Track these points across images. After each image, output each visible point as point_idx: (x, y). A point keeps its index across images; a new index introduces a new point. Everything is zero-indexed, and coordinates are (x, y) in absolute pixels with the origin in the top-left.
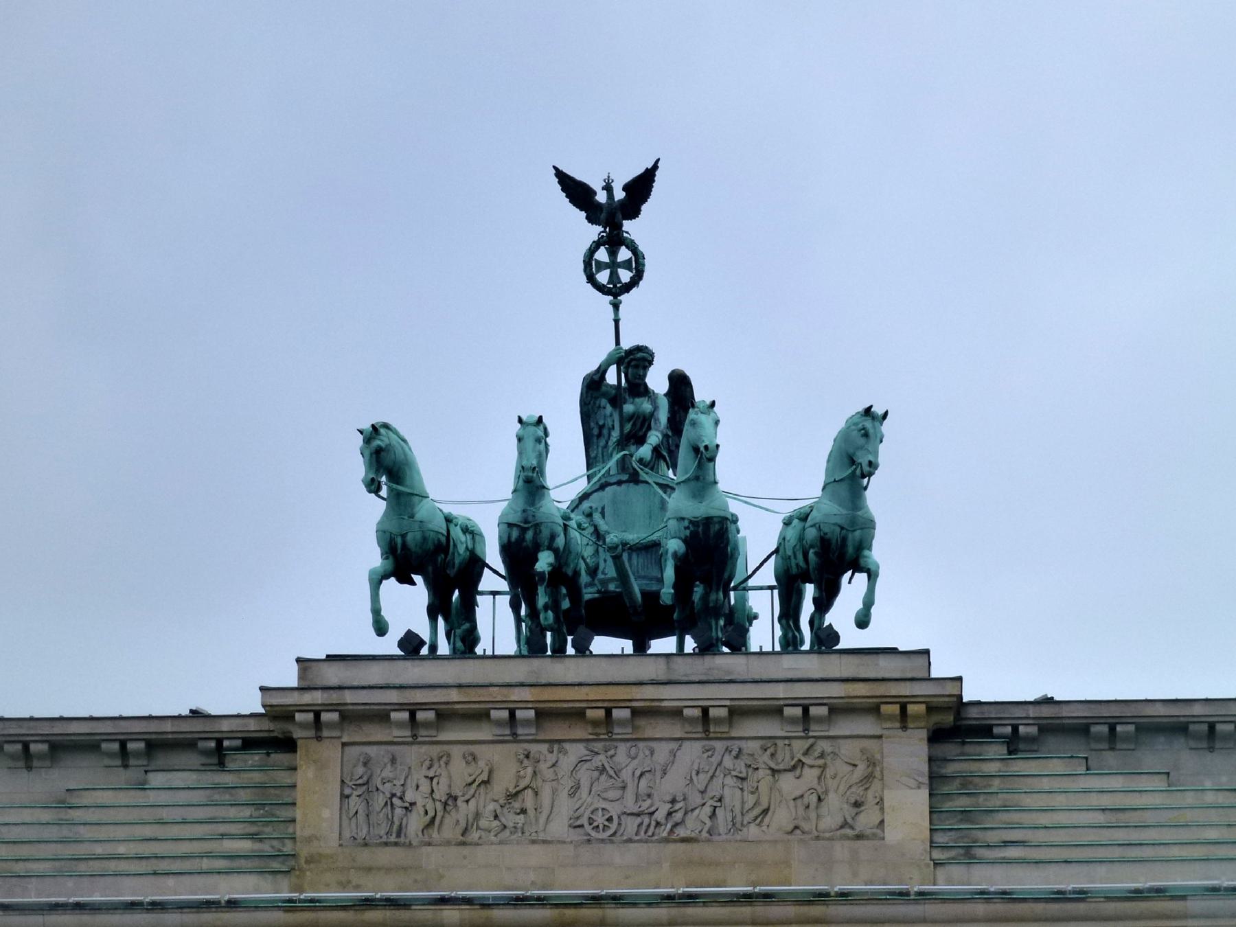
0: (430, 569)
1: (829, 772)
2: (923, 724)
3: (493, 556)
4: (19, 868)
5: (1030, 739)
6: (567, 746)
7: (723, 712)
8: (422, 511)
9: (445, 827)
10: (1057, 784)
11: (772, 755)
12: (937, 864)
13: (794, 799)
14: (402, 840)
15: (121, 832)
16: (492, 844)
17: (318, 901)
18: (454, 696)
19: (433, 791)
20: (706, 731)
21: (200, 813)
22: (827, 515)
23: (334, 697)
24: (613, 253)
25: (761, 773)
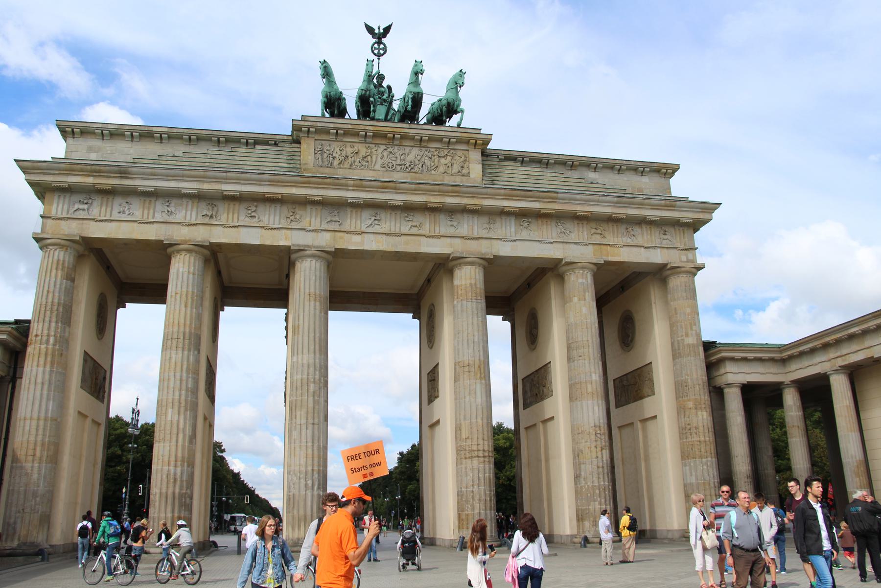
0: (337, 103)
2: (480, 147)
4: (217, 165)
6: (380, 146)
7: (427, 138)
11: (439, 153)
16: (359, 169)
18: (350, 126)
19: (341, 154)
23: (314, 124)
24: (379, 46)
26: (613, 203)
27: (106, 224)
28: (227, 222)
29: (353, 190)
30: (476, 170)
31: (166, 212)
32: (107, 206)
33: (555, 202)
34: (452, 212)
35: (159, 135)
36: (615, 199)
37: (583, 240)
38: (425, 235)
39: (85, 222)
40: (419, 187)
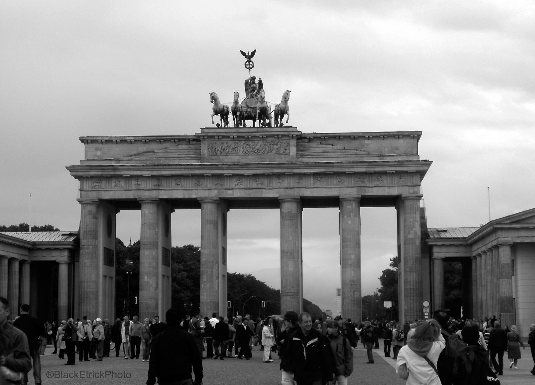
1: (282, 145)
3: (230, 111)
4: (159, 159)
5: (312, 139)
6: (242, 141)
8: (219, 105)
9: (223, 153)
10: (316, 146)
11: (273, 143)
12: (297, 158)
13: (276, 149)
14: (217, 155)
15: (174, 153)
17: (205, 164)
19: (221, 148)
20: (263, 139)
21: (187, 151)
22: (282, 106)
24: (249, 63)
25: (271, 145)
26: (366, 166)
27: (109, 192)
28: (167, 188)
29: (226, 170)
30: (293, 150)
31: (137, 185)
32: (109, 183)
33: (334, 168)
34: (279, 176)
35: (130, 141)
36: (367, 164)
37: (351, 185)
38: (265, 188)
39: (99, 191)
40: (259, 165)
